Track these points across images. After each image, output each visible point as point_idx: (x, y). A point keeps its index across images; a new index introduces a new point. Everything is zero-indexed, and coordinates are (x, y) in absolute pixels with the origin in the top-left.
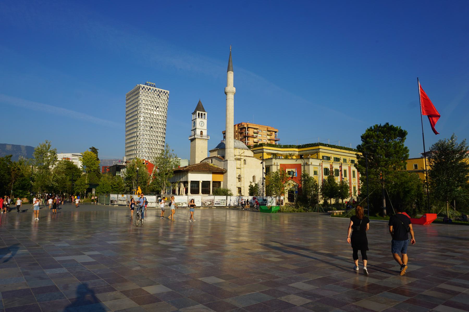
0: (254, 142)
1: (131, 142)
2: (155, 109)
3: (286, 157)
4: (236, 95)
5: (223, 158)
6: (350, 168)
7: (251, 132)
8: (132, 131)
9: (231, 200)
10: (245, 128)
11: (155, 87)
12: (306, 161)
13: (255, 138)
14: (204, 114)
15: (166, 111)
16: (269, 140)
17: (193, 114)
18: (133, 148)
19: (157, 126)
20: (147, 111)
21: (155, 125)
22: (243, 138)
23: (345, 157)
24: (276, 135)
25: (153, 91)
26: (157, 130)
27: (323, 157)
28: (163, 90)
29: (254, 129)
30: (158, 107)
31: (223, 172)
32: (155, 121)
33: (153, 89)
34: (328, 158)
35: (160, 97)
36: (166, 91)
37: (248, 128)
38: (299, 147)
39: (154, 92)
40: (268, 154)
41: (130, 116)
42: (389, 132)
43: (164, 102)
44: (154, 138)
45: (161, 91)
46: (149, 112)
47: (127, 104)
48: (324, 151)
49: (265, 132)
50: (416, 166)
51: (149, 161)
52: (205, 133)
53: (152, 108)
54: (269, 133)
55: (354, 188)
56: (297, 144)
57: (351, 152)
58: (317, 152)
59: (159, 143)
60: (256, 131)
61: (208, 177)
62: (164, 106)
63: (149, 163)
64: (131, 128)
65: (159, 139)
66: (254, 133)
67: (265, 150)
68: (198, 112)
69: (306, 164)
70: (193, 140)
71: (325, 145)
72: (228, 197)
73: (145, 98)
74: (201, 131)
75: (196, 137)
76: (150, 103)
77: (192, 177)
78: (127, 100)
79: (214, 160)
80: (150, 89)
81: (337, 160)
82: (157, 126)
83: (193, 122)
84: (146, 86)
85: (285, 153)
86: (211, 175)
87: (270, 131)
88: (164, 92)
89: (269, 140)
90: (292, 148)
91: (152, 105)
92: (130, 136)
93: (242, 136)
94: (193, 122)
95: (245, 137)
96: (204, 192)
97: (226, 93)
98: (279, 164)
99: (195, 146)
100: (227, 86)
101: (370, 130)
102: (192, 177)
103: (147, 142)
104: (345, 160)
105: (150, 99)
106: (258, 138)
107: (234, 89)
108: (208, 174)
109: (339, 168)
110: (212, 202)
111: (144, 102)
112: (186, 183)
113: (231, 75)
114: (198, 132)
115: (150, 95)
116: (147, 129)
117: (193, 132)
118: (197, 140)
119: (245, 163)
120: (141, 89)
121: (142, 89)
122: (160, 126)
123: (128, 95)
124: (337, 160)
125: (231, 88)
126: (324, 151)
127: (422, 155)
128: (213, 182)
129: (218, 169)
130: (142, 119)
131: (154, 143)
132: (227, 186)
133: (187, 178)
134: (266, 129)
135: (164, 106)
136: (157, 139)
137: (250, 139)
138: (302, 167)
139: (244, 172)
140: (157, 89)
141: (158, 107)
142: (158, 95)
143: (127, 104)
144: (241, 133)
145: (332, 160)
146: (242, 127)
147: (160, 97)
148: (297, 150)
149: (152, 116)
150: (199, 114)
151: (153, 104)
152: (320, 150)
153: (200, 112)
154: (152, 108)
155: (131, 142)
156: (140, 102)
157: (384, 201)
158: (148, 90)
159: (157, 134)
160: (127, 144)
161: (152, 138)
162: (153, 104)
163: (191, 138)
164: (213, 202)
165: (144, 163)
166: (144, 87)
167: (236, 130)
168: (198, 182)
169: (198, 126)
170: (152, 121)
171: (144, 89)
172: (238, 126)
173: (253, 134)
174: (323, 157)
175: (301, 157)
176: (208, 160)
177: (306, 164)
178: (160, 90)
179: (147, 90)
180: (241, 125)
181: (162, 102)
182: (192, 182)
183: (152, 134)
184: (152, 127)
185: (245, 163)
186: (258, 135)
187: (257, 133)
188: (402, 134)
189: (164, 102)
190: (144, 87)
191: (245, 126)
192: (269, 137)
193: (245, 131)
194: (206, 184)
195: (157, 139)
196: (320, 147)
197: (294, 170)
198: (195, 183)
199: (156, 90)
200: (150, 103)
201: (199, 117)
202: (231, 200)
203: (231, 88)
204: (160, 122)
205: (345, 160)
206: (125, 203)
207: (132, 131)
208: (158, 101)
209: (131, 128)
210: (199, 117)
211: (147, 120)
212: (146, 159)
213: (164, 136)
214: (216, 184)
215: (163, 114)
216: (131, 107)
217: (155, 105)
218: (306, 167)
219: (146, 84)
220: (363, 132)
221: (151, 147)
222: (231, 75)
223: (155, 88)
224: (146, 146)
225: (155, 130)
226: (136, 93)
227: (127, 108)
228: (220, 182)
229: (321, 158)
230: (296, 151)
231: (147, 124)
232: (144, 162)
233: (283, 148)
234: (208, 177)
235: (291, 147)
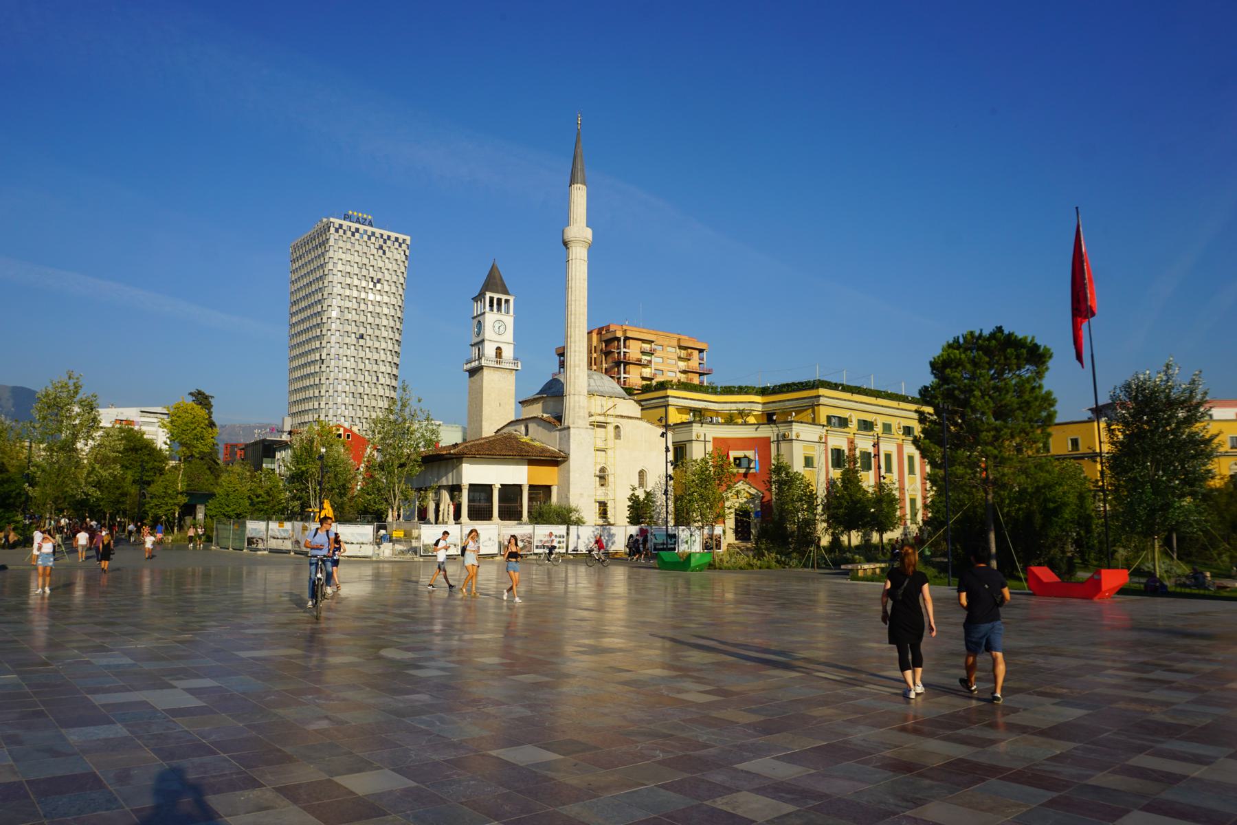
0: (644, 378)
1: (303, 378)
3: (730, 420)
4: (593, 249)
5: (557, 420)
6: (900, 449)
7: (634, 350)
8: (307, 348)
9: (578, 537)
10: (618, 339)
11: (370, 224)
12: (783, 429)
13: (644, 366)
14: (507, 301)
15: (401, 291)
16: (684, 372)
17: (476, 299)
18: (310, 393)
19: (377, 333)
20: (348, 292)
22: (612, 368)
23: (888, 420)
24: (702, 359)
25: (365, 238)
26: (377, 345)
27: (829, 418)
28: (394, 235)
30: (379, 281)
31: (556, 460)
32: (370, 320)
33: (366, 231)
34: (843, 422)
35: (384, 253)
36: (401, 237)
37: (627, 339)
38: (764, 391)
39: (369, 238)
40: (681, 410)
41: (303, 304)
42: (1006, 352)
43: (396, 267)
45: (389, 237)
46: (355, 294)
47: (293, 272)
49: (673, 352)
50: (1075, 442)
51: (355, 429)
52: (508, 353)
53: (364, 284)
54: (683, 353)
55: (913, 501)
58: (813, 405)
59: (382, 380)
60: (647, 347)
61: (518, 475)
62: (395, 278)
64: (304, 337)
65: (383, 369)
66: (643, 353)
67: (671, 401)
68: (488, 295)
69: (784, 438)
70: (474, 372)
71: (834, 387)
72: (573, 529)
73: (343, 256)
74: (499, 348)
75: (483, 363)
76: (357, 271)
77: (473, 473)
78: (294, 261)
79: (532, 426)
80: (357, 230)
81: (866, 426)
84: (346, 224)
85: (727, 407)
87: (685, 348)
88: (397, 239)
89: (684, 372)
90: (746, 393)
91: (364, 276)
92: (302, 361)
93: (610, 360)
95: (618, 364)
96: (504, 515)
97: (565, 244)
98: (709, 438)
100: (568, 224)
101: (954, 345)
102: (473, 473)
103: (348, 376)
104: (887, 428)
107: (588, 234)
109: (871, 450)
111: (340, 267)
112: (455, 489)
113: (579, 196)
114: (489, 350)
115: (357, 247)
117: (475, 350)
118: (485, 371)
120: (332, 230)
121: (337, 231)
122: (385, 334)
123: (295, 249)
124: (866, 426)
125: (579, 230)
126: (831, 402)
127: (1090, 414)
128: (531, 487)
129: (544, 450)
130: (334, 314)
131: (368, 379)
132: (567, 498)
133: (460, 476)
134: (675, 343)
135: (395, 278)
136: (375, 368)
137: (632, 368)
139: (615, 459)
140: (378, 231)
141: (379, 281)
142: (381, 247)
143: (293, 272)
144: (607, 354)
145: (854, 425)
146: (610, 336)
147: (384, 253)
148: (758, 399)
149: (363, 307)
150: (491, 300)
151: (364, 272)
152: (822, 400)
153: (496, 296)
154: (364, 284)
155: (303, 378)
156: (330, 266)
157: (992, 536)
158: (353, 235)
159: (376, 356)
160: (292, 382)
161: (361, 366)
162: (364, 272)
163: (469, 366)
164: (530, 543)
165: (340, 436)
167: (594, 344)
168: (489, 487)
169: (489, 333)
170: (363, 319)
171: (341, 231)
172: (599, 333)
173: (640, 356)
174: (829, 418)
175: (769, 418)
176: (517, 427)
177: (784, 438)
178: (386, 233)
179: (349, 234)
180: (608, 331)
181: (390, 266)
182: (472, 487)
183: (362, 354)
184: (362, 337)
186: (654, 359)
187: (651, 353)
190: (341, 226)
191: (619, 334)
192: (682, 365)
193: (619, 348)
194: (510, 493)
195: (375, 368)
196: (822, 391)
197: (750, 454)
199: (373, 234)
200: (357, 271)
201: (492, 310)
202: (578, 537)
203: (579, 230)
204: (385, 322)
205: (887, 428)
206: (288, 545)
207: (307, 348)
208: (381, 264)
209: (304, 337)
210: (492, 310)
211: (349, 316)
212: (346, 425)
213: (396, 360)
214: (540, 492)
215: (394, 301)
216: (305, 281)
217: (372, 274)
218: (783, 445)
219: (347, 217)
220: (936, 351)
222: (579, 196)
223: (370, 229)
224: (347, 389)
225: (369, 343)
226: (319, 241)
227: (292, 282)
229: (823, 420)
230: (756, 403)
231: (349, 328)
232: (341, 431)
233: (721, 394)
234: (518, 475)
235: (742, 390)
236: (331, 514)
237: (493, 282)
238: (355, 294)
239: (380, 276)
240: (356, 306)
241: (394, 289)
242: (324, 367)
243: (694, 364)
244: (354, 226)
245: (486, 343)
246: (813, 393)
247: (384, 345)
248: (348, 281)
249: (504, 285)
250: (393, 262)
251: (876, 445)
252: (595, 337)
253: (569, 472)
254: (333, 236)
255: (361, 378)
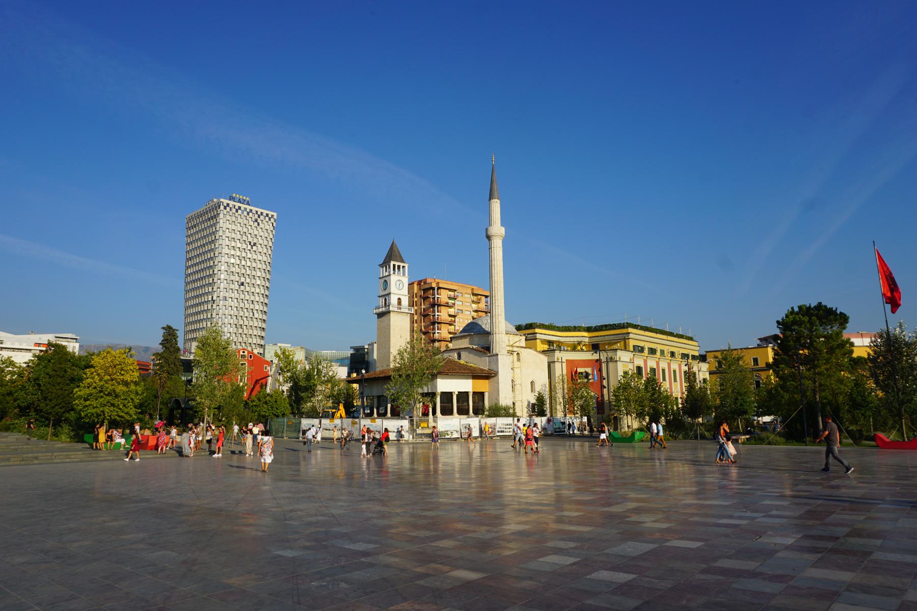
0: (450, 316)
1: (197, 313)
2: (249, 247)
3: (574, 348)
5: (487, 349)
6: (669, 365)
7: (443, 296)
10: (433, 289)
11: (248, 204)
12: (610, 354)
13: (450, 307)
16: (476, 311)
17: (381, 266)
20: (233, 252)
21: (248, 280)
22: (429, 308)
24: (487, 302)
25: (245, 213)
27: (634, 346)
28: (265, 212)
29: (450, 290)
30: (255, 244)
31: (489, 375)
32: (249, 272)
33: (246, 209)
34: (642, 350)
36: (270, 213)
37: (439, 288)
39: (248, 214)
42: (825, 317)
43: (266, 235)
44: (247, 306)
45: (262, 213)
46: (238, 253)
48: (636, 337)
49: (469, 297)
50: (756, 360)
51: (255, 352)
52: (405, 302)
53: (244, 246)
54: (475, 298)
56: (560, 325)
57: (670, 338)
58: (625, 339)
59: (256, 315)
60: (452, 294)
62: (266, 243)
63: (255, 355)
64: (198, 284)
65: (257, 307)
66: (450, 298)
67: (538, 336)
68: (392, 263)
70: (383, 315)
71: (636, 327)
73: (230, 226)
74: (399, 299)
77: (444, 385)
78: (188, 229)
79: (463, 354)
80: (240, 208)
81: (652, 351)
82: (253, 281)
83: (382, 280)
84: (231, 203)
86: (471, 381)
87: (477, 295)
88: (267, 215)
89: (476, 311)
90: (579, 331)
91: (243, 240)
92: (197, 301)
93: (427, 303)
94: (382, 280)
95: (433, 305)
97: (489, 237)
98: (564, 360)
99: (389, 325)
100: (490, 225)
101: (792, 312)
102: (444, 385)
103: (232, 313)
104: (662, 352)
105: (240, 229)
106: (456, 307)
107: (502, 231)
108: (467, 378)
109: (655, 367)
110: (493, 427)
111: (228, 234)
112: (433, 395)
113: (496, 205)
114: (394, 300)
115: (240, 220)
116: (232, 286)
117: (382, 300)
118: (392, 314)
119: (519, 360)
120: (222, 207)
121: (225, 208)
122: (258, 282)
123: (190, 219)
124: (652, 351)
125: (498, 230)
126: (636, 337)
127: (759, 342)
129: (482, 370)
132: (498, 399)
134: (470, 291)
135: (266, 243)
137: (443, 309)
138: (604, 366)
139: (523, 375)
140: (254, 209)
142: (256, 220)
144: (425, 298)
145: (646, 351)
146: (427, 286)
148: (586, 334)
149: (243, 263)
150: (394, 266)
151: (245, 238)
152: (631, 336)
153: (397, 264)
154: (244, 246)
155: (197, 313)
156: (221, 233)
157: (820, 419)
158: (237, 211)
159: (252, 298)
161: (242, 305)
162: (245, 238)
166: (228, 205)
167: (415, 291)
168: (451, 394)
169: (393, 288)
170: (243, 271)
171: (228, 209)
172: (419, 283)
174: (634, 346)
175: (595, 347)
176: (451, 354)
178: (260, 210)
179: (234, 210)
180: (425, 283)
181: (262, 234)
182: (443, 394)
183: (242, 296)
184: (242, 284)
185: (519, 360)
188: (843, 319)
189: (266, 235)
190: (228, 205)
191: (434, 285)
192: (475, 306)
193: (433, 294)
194: (463, 396)
196: (630, 330)
197: (589, 370)
198: (447, 396)
199: (251, 211)
200: (239, 237)
203: (498, 230)
204: (259, 274)
205: (662, 352)
208: (256, 232)
209: (198, 284)
211: (233, 269)
212: (250, 349)
213: (266, 301)
214: (479, 396)
215: (265, 259)
218: (611, 364)
219: (231, 198)
220: (780, 316)
221: (241, 322)
222: (496, 205)
223: (249, 208)
224: (232, 321)
225: (248, 289)
226: (211, 215)
227: (188, 244)
228: (482, 394)
229: (631, 349)
230: (585, 337)
231: (233, 278)
233: (562, 331)
235: (575, 329)
236: (344, 415)
237: (392, 255)
238: (238, 253)
239: (255, 241)
240: (238, 262)
241: (265, 251)
242: (214, 306)
243: (482, 306)
244: (237, 205)
245: (392, 295)
246: (624, 331)
247: (258, 290)
248: (233, 244)
249: (401, 257)
250: (264, 232)
251: (658, 363)
252: (415, 286)
253: (498, 383)
254: (222, 211)
255: (241, 314)
